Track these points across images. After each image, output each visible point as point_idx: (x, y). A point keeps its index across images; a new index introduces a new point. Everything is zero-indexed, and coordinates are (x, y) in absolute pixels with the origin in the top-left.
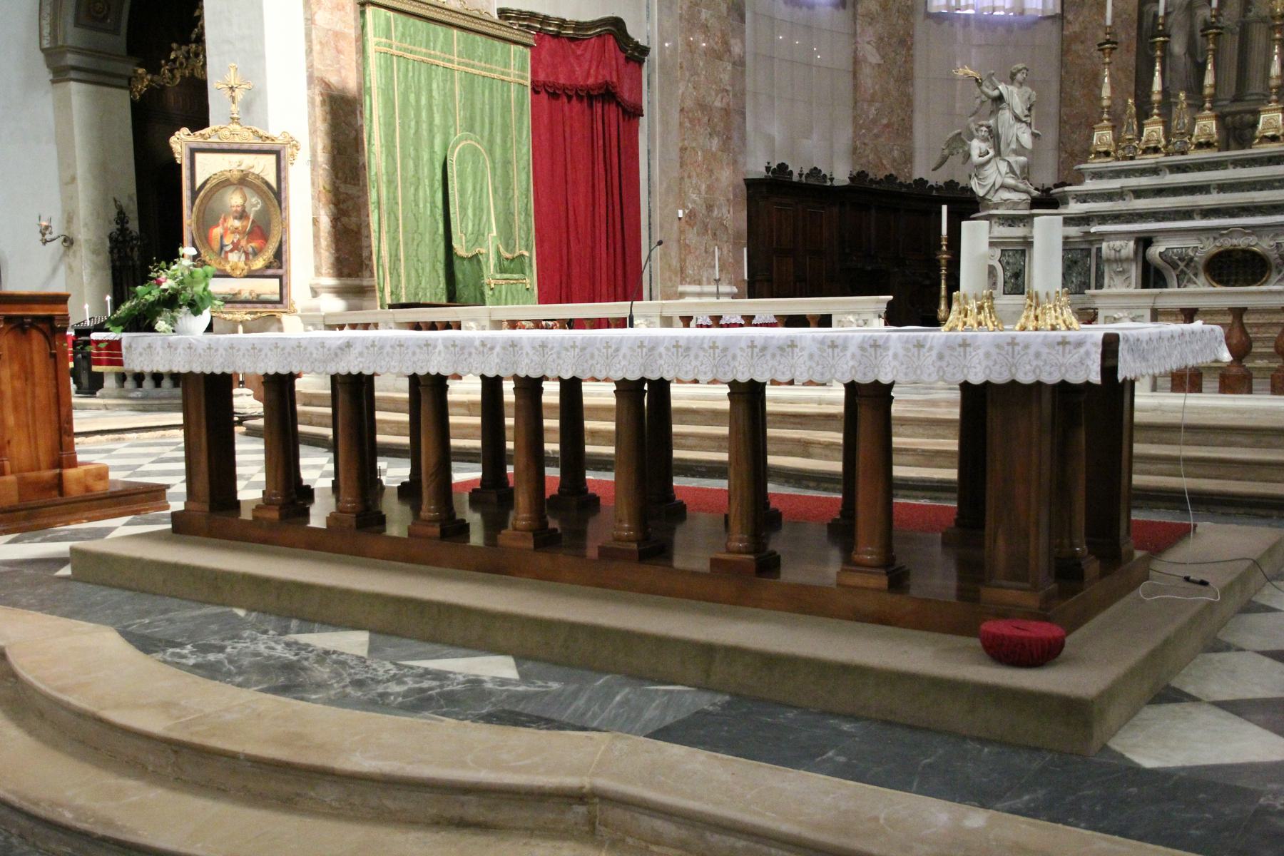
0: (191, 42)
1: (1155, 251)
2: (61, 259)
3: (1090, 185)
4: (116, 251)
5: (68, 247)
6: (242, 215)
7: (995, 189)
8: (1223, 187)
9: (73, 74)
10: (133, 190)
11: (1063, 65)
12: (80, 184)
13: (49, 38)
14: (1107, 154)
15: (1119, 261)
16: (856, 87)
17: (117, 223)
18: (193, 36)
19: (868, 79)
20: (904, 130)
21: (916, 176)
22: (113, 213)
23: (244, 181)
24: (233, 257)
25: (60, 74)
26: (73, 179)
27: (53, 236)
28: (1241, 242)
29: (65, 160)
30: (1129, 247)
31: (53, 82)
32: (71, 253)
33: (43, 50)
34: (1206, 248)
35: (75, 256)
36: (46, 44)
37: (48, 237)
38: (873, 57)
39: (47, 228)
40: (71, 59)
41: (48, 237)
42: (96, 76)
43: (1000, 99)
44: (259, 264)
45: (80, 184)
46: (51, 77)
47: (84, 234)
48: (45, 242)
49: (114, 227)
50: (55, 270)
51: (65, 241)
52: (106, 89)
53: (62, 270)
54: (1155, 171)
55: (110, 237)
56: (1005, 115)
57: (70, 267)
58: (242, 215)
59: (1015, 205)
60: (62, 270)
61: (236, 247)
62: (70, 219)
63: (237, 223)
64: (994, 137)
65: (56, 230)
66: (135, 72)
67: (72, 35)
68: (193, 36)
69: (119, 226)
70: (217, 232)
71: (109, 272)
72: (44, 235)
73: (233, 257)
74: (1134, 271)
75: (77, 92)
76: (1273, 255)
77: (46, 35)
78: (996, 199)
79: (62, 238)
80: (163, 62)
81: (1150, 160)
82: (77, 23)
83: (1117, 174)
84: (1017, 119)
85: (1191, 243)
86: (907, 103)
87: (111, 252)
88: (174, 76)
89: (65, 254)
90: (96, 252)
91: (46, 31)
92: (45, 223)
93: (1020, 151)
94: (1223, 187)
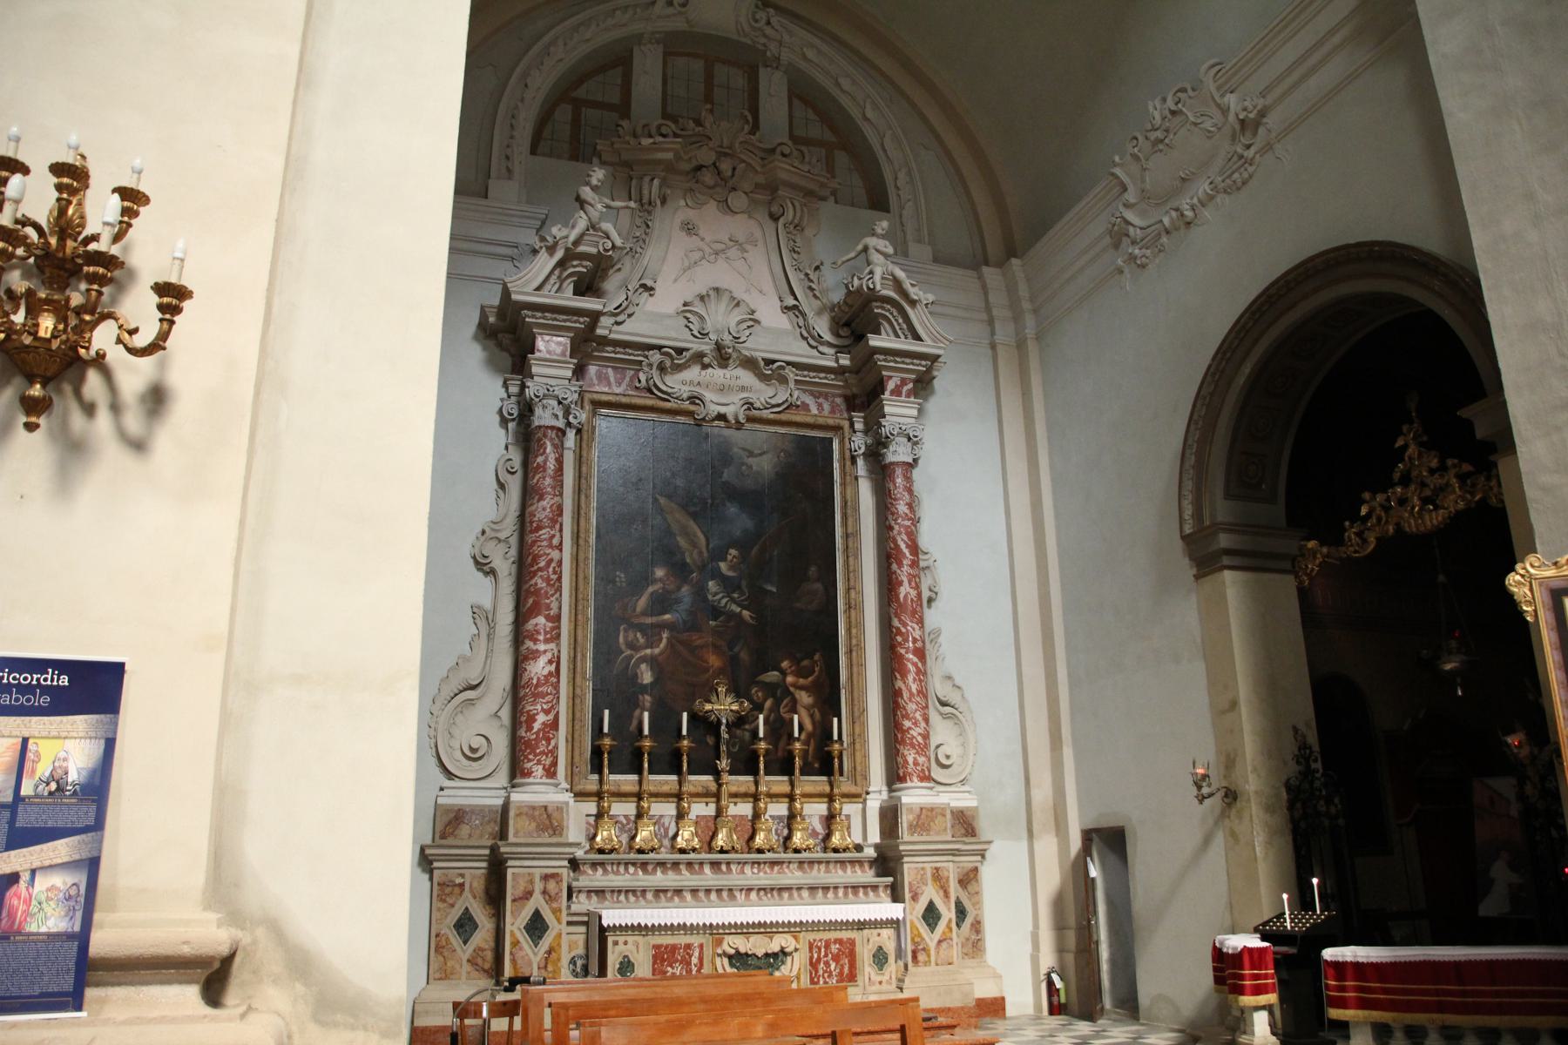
0: (1396, 484)
2: (1216, 823)
4: (1299, 805)
5: (1229, 805)
9: (1226, 560)
10: (1313, 716)
12: (1244, 710)
13: (1191, 521)
17: (1298, 763)
18: (1396, 476)
22: (1291, 748)
25: (1205, 561)
26: (1234, 705)
27: (1214, 788)
29: (1218, 679)
31: (1197, 577)
32: (1234, 811)
33: (1184, 538)
35: (1240, 818)
36: (1188, 530)
37: (1205, 790)
39: (1205, 777)
40: (1224, 540)
41: (1205, 790)
42: (1253, 561)
45: (1244, 710)
46: (1194, 571)
47: (1254, 781)
48: (1201, 799)
49: (1293, 768)
50: (1207, 841)
51: (1226, 795)
52: (1266, 576)
53: (1219, 840)
55: (1288, 785)
57: (1233, 835)
60: (1219, 840)
62: (1229, 762)
65: (1217, 782)
66: (1301, 548)
67: (1221, 509)
68: (1396, 476)
69: (1301, 768)
71: (1289, 838)
72: (1199, 788)
75: (1232, 583)
77: (1187, 517)
79: (1222, 793)
80: (1347, 523)
82: (1228, 495)
87: (1291, 806)
88: (1365, 541)
89: (1223, 815)
90: (1269, 809)
91: (1188, 511)
92: (1200, 771)
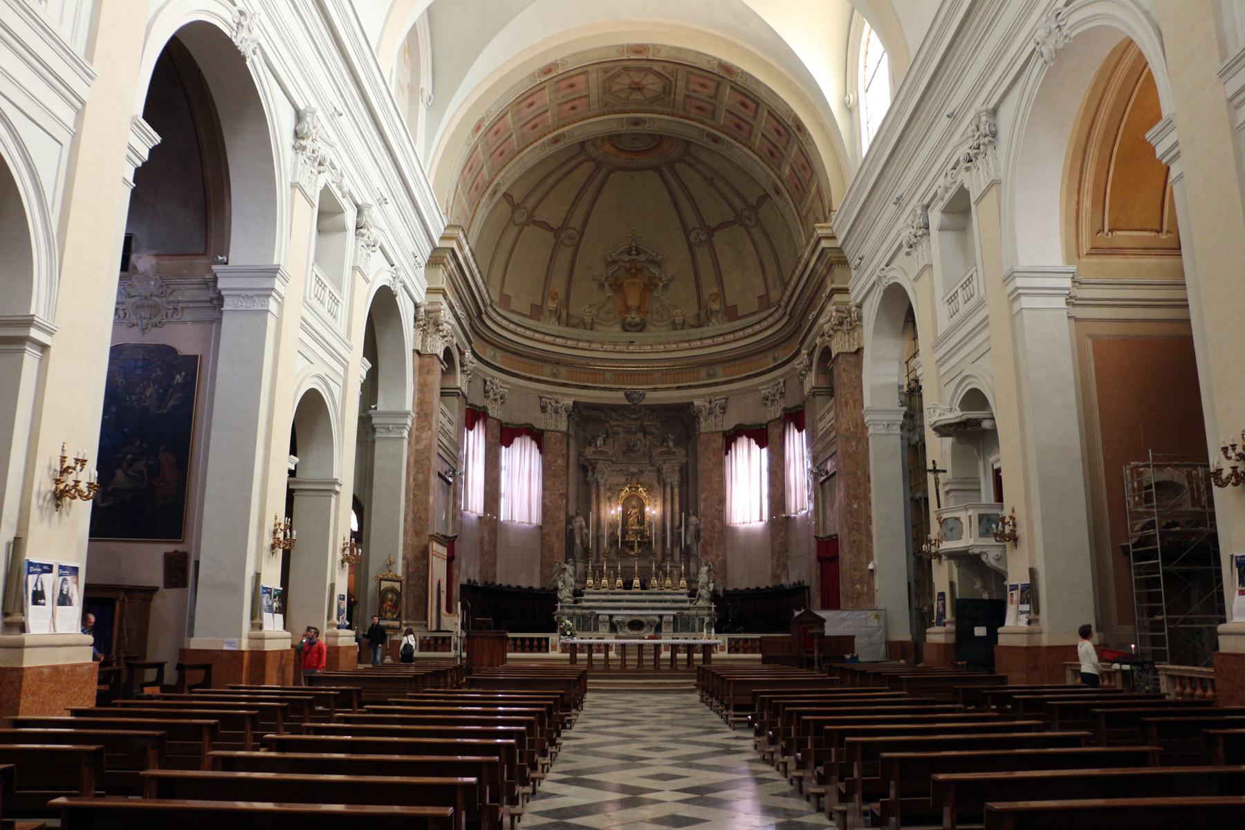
1: (615, 619)
3: (586, 597)
6: (391, 601)
7: (565, 597)
8: (628, 601)
11: (542, 544)
14: (591, 587)
15: (604, 622)
16: (482, 548)
19: (486, 548)
20: (494, 565)
21: (498, 583)
23: (392, 590)
24: (389, 614)
28: (638, 618)
30: (607, 618)
34: (629, 619)
38: (487, 538)
43: (565, 569)
44: (395, 616)
54: (606, 594)
56: (567, 575)
58: (391, 601)
59: (570, 602)
61: (390, 611)
63: (389, 603)
64: (564, 582)
70: (385, 605)
73: (389, 614)
74: (608, 625)
76: (645, 622)
78: (565, 600)
81: (604, 590)
83: (595, 594)
84: (571, 576)
85: (624, 617)
86: (495, 554)
93: (571, 585)
94: (628, 601)
